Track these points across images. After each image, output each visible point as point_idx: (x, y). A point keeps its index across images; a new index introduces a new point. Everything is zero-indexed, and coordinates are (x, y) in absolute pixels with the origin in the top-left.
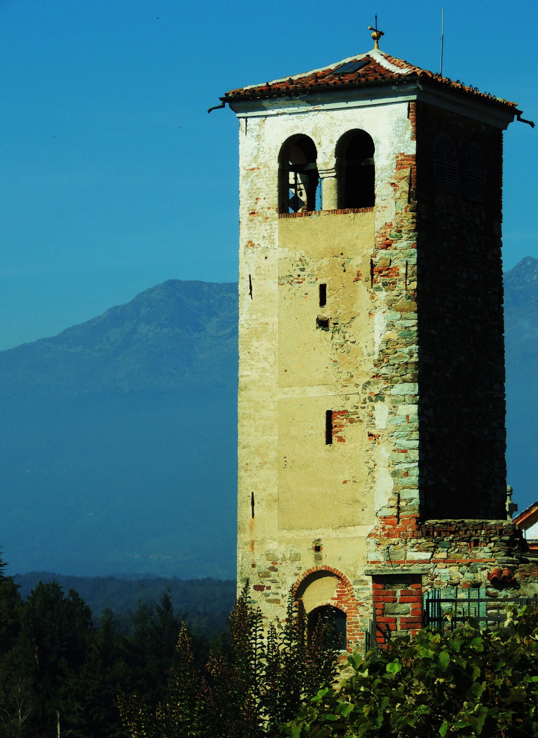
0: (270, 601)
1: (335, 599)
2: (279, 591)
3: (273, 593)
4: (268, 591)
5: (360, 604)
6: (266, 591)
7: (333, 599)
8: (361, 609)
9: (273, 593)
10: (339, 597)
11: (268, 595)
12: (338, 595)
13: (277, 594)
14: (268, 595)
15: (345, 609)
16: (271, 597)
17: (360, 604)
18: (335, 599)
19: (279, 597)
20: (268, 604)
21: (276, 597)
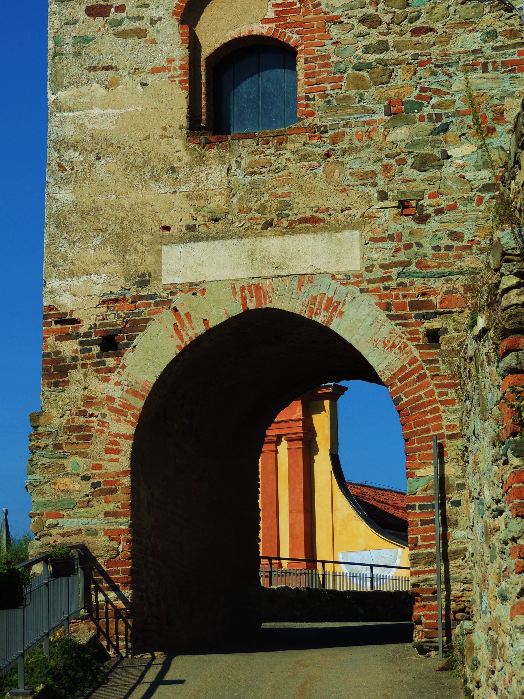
0: (123, 35)
1: (270, 21)
2: (146, 13)
3: (131, 19)
4: (119, 16)
5: (335, 21)
6: (113, 15)
7: (264, 21)
8: (334, 31)
9: (131, 19)
10: (280, 16)
11: (119, 23)
12: (277, 13)
13: (140, 18)
14: (119, 23)
15: (292, 37)
16: (127, 25)
17: (335, 21)
18: (270, 21)
19: (144, 24)
20: (119, 41)
21: (137, 25)
